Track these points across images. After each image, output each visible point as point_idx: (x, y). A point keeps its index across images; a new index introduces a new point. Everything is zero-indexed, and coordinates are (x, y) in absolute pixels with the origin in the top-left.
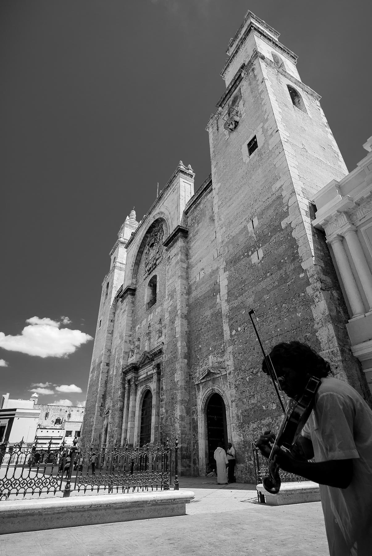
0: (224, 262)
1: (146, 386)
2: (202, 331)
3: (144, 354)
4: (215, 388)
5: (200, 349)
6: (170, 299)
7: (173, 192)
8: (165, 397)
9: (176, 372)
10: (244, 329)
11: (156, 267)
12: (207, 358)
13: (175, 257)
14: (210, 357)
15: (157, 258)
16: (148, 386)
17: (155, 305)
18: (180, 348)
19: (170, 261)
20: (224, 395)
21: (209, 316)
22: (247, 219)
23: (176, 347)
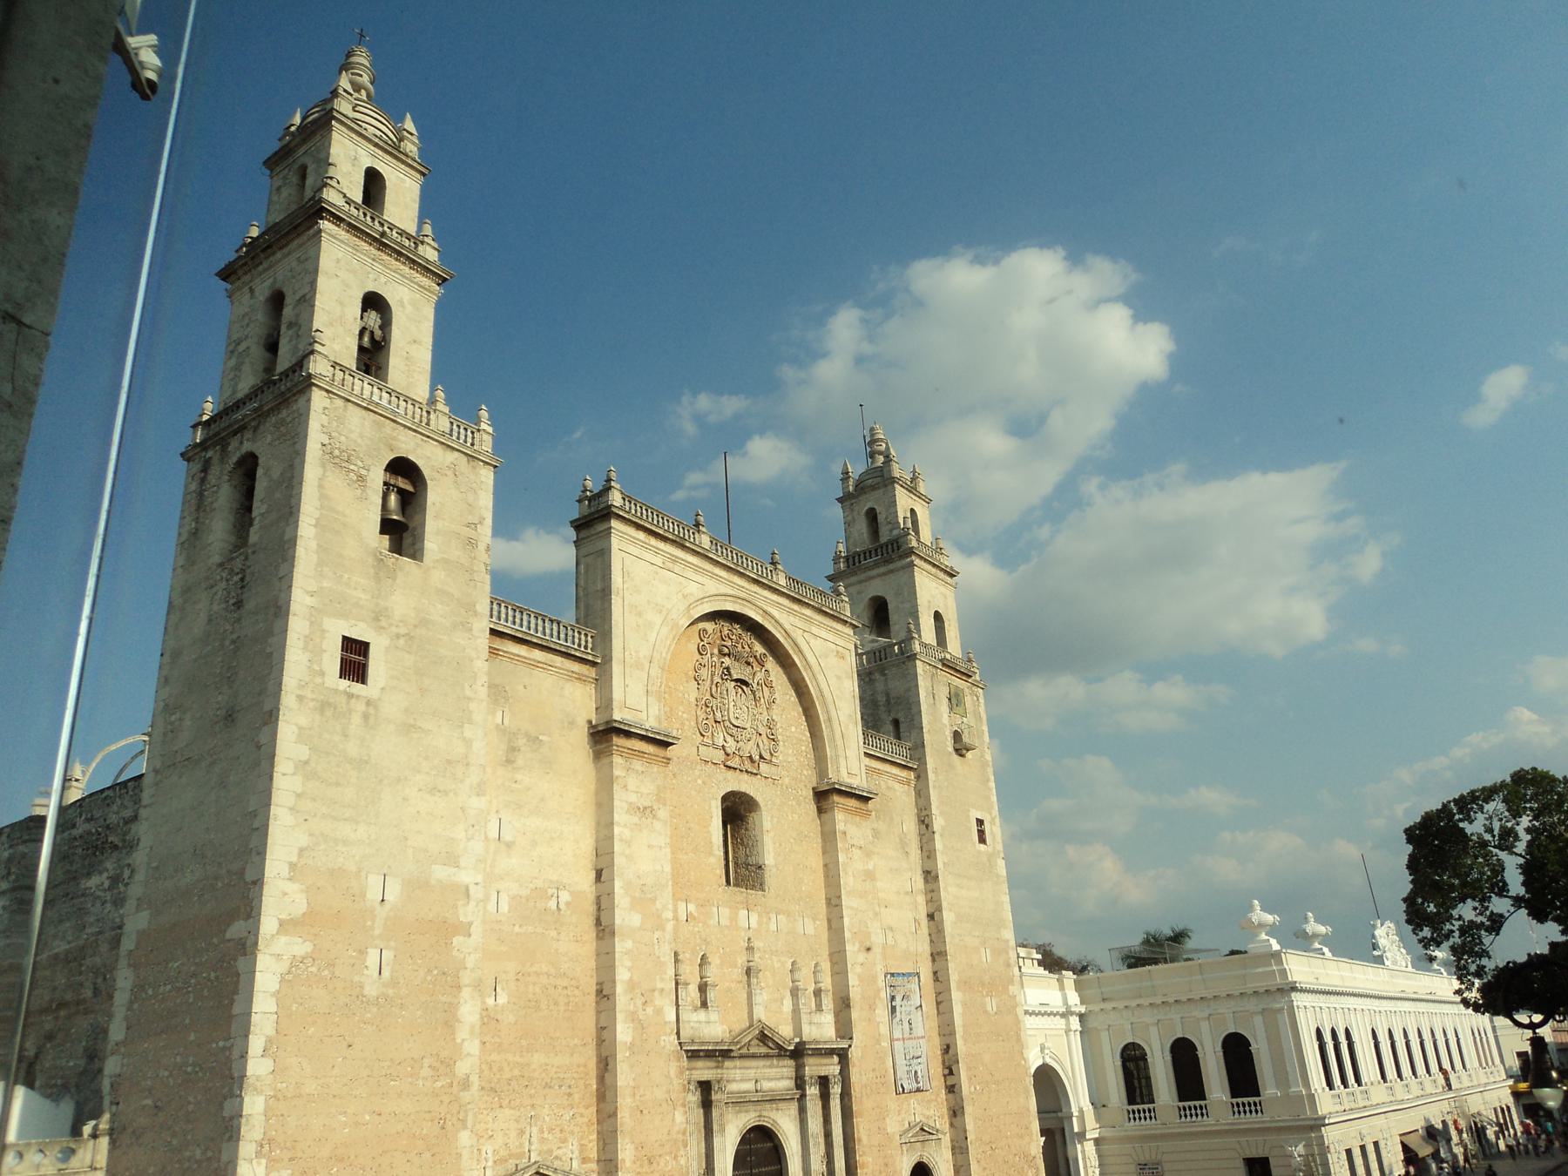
6: (857, 945)
8: (870, 1159)
9: (888, 1115)
11: (757, 774)
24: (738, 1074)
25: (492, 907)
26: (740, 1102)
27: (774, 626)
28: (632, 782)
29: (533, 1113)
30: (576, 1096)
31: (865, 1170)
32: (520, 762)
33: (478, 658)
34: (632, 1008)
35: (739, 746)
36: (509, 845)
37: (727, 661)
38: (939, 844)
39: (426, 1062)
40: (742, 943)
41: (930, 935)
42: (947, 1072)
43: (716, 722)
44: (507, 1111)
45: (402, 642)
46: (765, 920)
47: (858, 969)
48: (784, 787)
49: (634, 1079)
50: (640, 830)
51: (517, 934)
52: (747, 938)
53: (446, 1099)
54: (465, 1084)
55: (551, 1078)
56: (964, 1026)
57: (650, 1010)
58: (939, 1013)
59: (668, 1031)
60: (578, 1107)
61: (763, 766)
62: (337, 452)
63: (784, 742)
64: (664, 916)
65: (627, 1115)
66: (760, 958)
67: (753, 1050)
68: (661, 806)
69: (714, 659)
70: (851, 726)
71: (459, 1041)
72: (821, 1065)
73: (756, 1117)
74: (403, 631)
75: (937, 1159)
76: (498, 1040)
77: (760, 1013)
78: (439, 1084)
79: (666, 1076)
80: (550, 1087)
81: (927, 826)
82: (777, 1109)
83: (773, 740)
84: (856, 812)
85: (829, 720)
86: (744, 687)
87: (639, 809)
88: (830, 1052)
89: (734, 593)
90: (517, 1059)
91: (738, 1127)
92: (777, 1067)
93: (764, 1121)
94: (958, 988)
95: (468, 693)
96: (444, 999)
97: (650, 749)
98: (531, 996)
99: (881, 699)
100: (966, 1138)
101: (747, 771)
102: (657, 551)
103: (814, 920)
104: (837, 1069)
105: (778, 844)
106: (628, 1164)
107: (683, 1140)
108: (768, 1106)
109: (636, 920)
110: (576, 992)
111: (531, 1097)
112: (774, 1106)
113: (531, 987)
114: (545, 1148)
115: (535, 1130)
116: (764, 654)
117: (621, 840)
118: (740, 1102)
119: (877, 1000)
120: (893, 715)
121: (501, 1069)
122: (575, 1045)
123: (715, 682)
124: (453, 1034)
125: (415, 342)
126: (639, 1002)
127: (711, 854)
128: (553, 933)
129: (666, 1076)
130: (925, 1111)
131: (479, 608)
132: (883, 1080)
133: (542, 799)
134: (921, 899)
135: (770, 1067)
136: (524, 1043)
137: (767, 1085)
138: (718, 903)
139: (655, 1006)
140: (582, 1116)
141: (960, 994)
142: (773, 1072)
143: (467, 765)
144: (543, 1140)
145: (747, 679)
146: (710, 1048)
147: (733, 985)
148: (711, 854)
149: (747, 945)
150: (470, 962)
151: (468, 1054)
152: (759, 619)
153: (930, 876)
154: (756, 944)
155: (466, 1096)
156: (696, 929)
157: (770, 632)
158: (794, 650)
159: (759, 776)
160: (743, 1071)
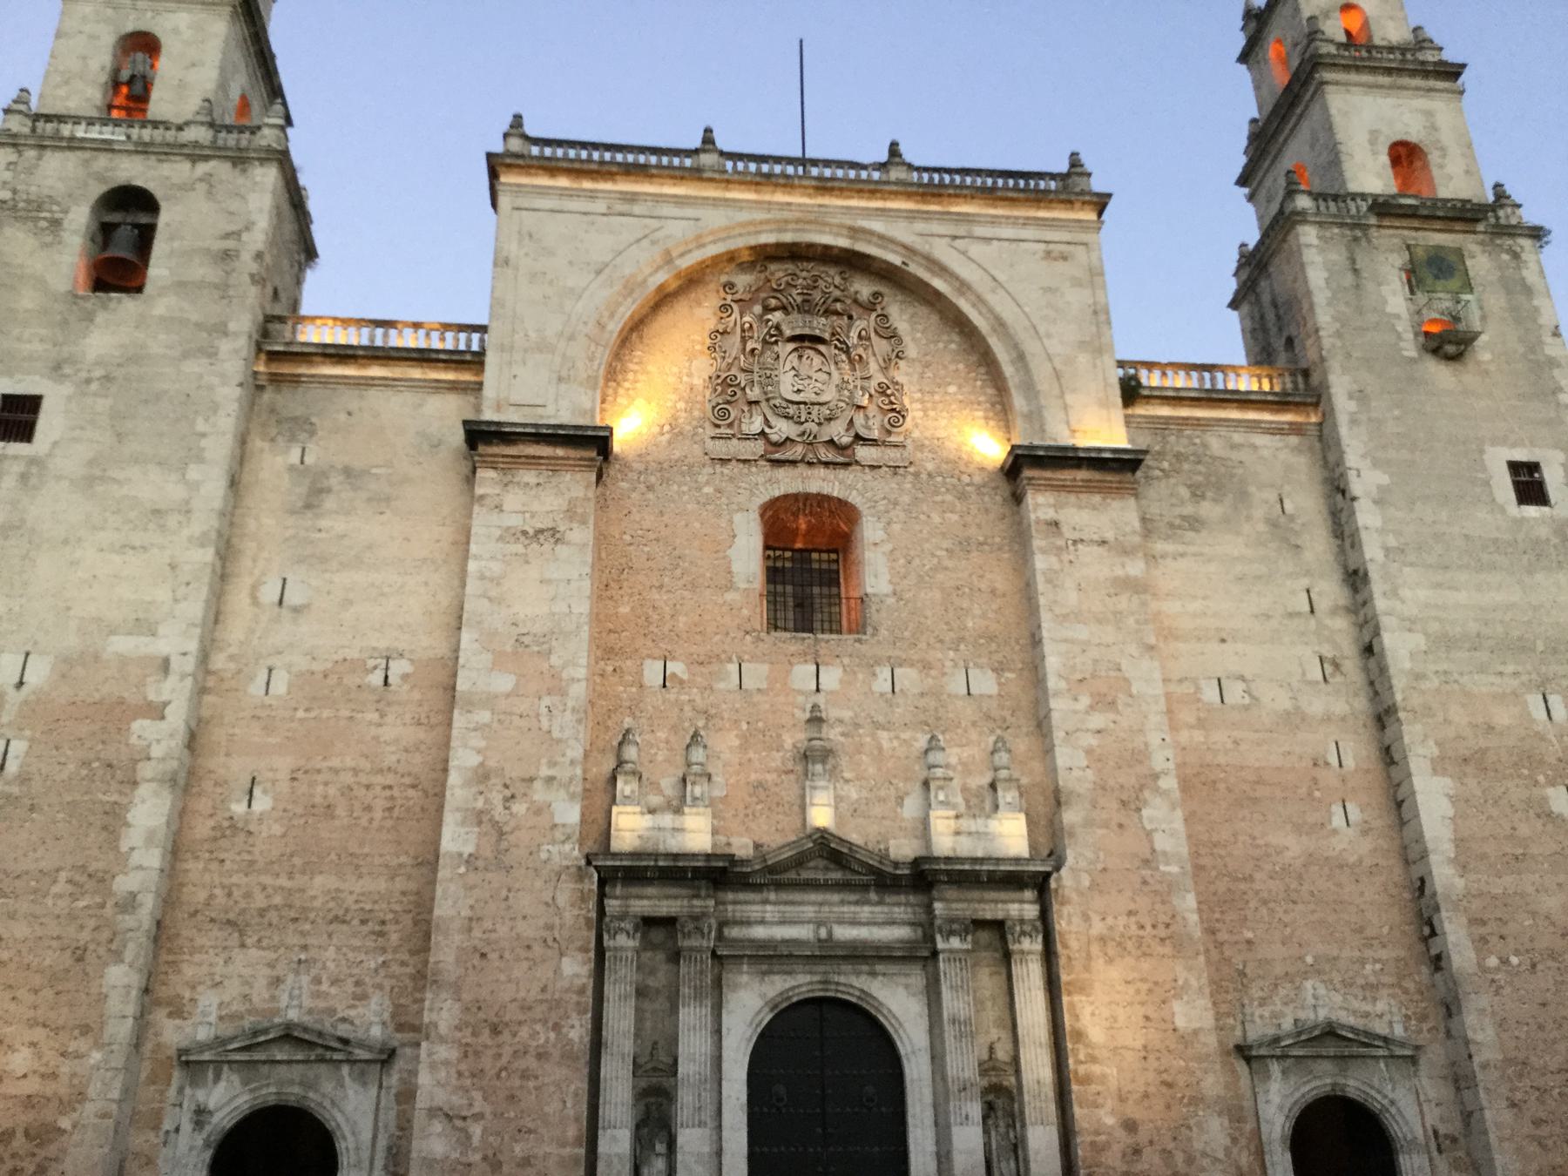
0: (1431, 743)
1: (820, 982)
2: (1257, 886)
4: (1351, 1082)
5: (1249, 942)
6: (1085, 701)
7: (1048, 255)
10: (1534, 966)
11: (846, 465)
12: (1292, 982)
13: (1096, 549)
14: (1308, 984)
15: (863, 433)
16: (838, 984)
17: (859, 641)
18: (1194, 918)
19: (1060, 542)
20: (1393, 1110)
21: (1289, 854)
22: (1525, 678)
23: (1163, 902)
24: (770, 911)
25: (257, 688)
26: (771, 957)
27: (880, 246)
28: (513, 499)
29: (303, 957)
30: (394, 938)
31: (1094, 1088)
32: (330, 503)
33: (224, 384)
34: (480, 804)
35: (802, 428)
36: (297, 610)
37: (777, 317)
38: (1366, 516)
39: (63, 876)
40: (798, 713)
41: (1372, 683)
42: (1427, 931)
43: (750, 403)
44: (253, 952)
45: (94, 386)
47: (1092, 741)
48: (924, 476)
49: (472, 907)
50: (527, 562)
51: (301, 720)
52: (809, 707)
53: (92, 923)
54: (129, 903)
55: (347, 910)
56: (1459, 842)
57: (519, 808)
58: (1402, 823)
59: (559, 835)
60: (395, 950)
61: (863, 453)
62: (21, 205)
64: (565, 675)
65: (451, 959)
66: (843, 734)
67: (806, 875)
68: (575, 525)
69: (747, 319)
70: (1083, 359)
71: (124, 848)
72: (981, 901)
73: (811, 983)
74: (98, 373)
75: (1391, 1095)
76: (246, 857)
77: (821, 816)
78: (81, 904)
79: (547, 904)
80: (344, 922)
81: (1343, 492)
82: (873, 974)
83: (893, 410)
84: (1088, 487)
85: (1021, 358)
86: (822, 348)
87: (524, 533)
88: (1010, 879)
89: (769, 216)
90: (283, 881)
91: (762, 996)
92: (880, 903)
94: (1435, 772)
95: (201, 426)
96: (105, 798)
97: (560, 452)
98: (318, 800)
99: (1270, 316)
100: (1470, 1057)
101: (820, 462)
102: (592, 195)
103: (998, 670)
104: (1031, 911)
105: (902, 561)
106: (443, 1028)
107: (578, 1003)
109: (503, 683)
110: (411, 793)
111: (303, 934)
112: (865, 968)
113: (320, 789)
114: (322, 1004)
115: (305, 980)
116: (876, 295)
117: (482, 577)
118: (771, 957)
119: (1147, 794)
120: (1285, 334)
121: (248, 895)
122: (400, 866)
124: (117, 839)
125: (193, 65)
126: (497, 798)
127: (730, 586)
128: (375, 716)
129: (547, 904)
130: (1356, 1004)
131: (232, 326)
132: (1162, 932)
133: (370, 547)
134: (1341, 624)
135: (857, 903)
136: (297, 861)
137: (843, 933)
138: (739, 658)
139: (533, 802)
140: (403, 964)
141: (1444, 783)
142: (865, 912)
143: (188, 512)
144: (317, 995)
145: (817, 332)
146: (661, 863)
147: (771, 777)
148: (730, 586)
149: (808, 715)
150: (156, 751)
151: (140, 868)
152: (843, 242)
153: (1356, 579)
154: (831, 713)
155: (128, 921)
156: (685, 698)
157: (868, 257)
158: (928, 269)
159: (854, 467)
160: (782, 908)
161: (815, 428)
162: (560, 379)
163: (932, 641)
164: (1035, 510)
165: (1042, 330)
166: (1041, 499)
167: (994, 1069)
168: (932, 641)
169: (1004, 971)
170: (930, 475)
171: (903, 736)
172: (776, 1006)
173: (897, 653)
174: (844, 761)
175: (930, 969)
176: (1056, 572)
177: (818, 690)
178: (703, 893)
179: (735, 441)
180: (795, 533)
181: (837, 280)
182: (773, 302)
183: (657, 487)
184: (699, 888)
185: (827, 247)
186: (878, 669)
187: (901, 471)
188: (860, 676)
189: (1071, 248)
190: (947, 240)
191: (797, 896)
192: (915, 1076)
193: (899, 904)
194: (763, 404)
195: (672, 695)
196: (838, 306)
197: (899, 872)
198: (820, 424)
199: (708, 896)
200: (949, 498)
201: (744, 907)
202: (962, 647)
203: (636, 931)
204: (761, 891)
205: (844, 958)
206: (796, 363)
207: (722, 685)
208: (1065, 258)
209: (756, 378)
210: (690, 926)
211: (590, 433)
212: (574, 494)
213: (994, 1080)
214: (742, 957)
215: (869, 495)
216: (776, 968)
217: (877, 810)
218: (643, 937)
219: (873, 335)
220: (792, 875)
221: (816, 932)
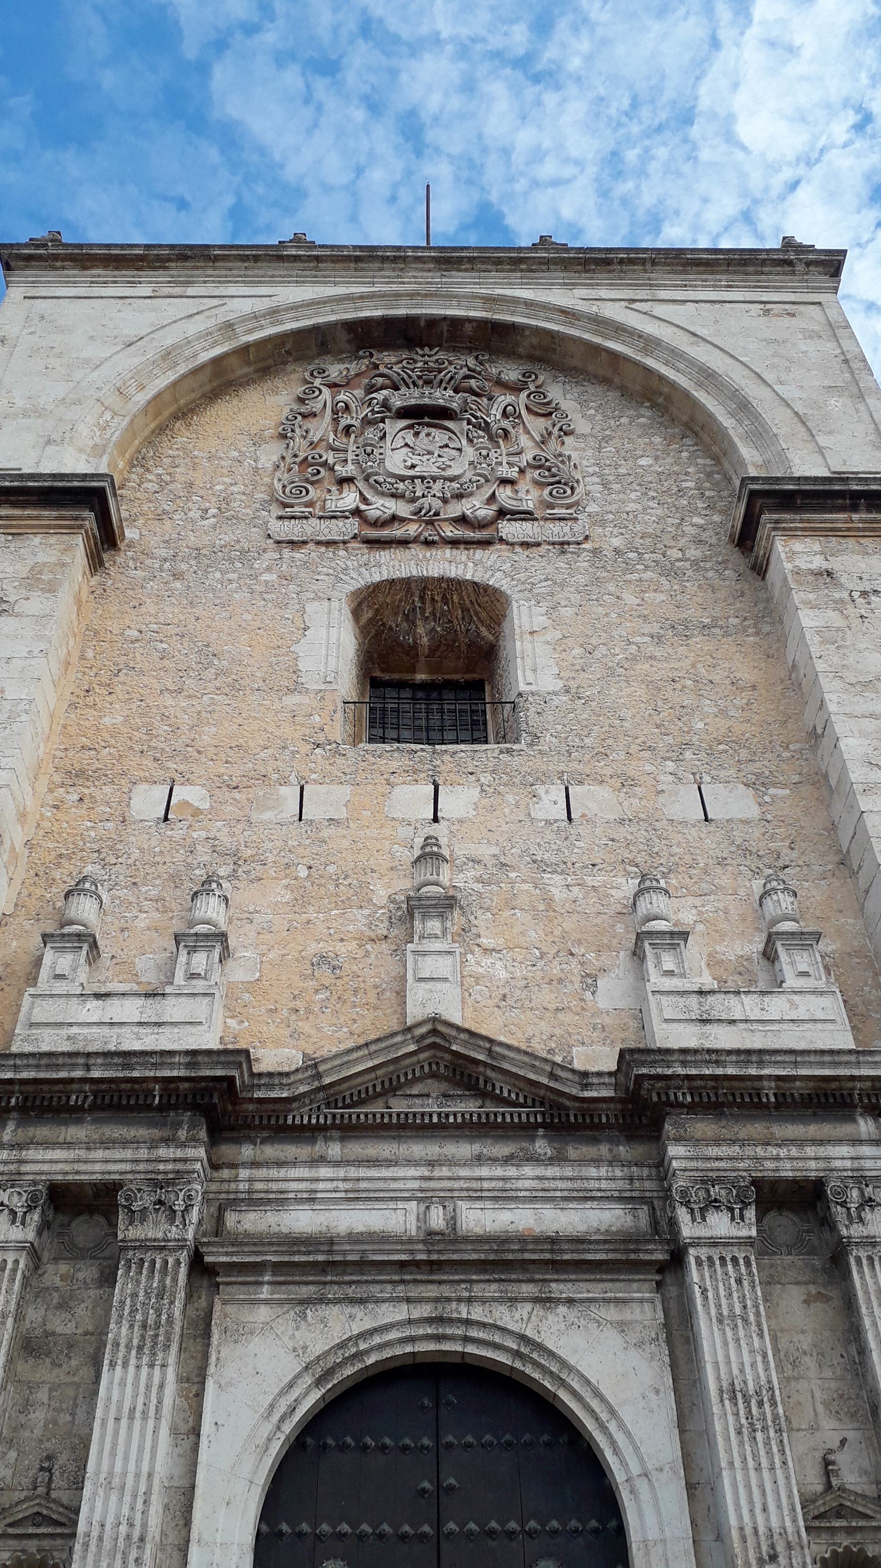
1: (429, 1321)
3: (423, 1030)
11: (486, 543)
16: (468, 1322)
17: (509, 751)
46: (510, 798)
48: (610, 554)
52: (419, 841)
63: (605, 485)
66: (479, 880)
67: (399, 1106)
69: (341, 397)
70: (836, 404)
82: (546, 1302)
83: (559, 482)
86: (450, 424)
93: (466, 1339)
105: (577, 651)
108: (492, 1290)
123: (340, 428)
135: (508, 1160)
146: (96, 1074)
147: (342, 949)
149: (417, 852)
160: (353, 1172)
161: (437, 504)
162: (49, 442)
163: (634, 749)
164: (790, 559)
165: (769, 377)
166: (797, 546)
167: (839, 1512)
168: (634, 749)
169: (834, 1293)
170: (617, 551)
171: (589, 881)
172: (329, 1373)
173: (575, 765)
174: (482, 920)
175: (672, 1291)
176: (838, 629)
177: (436, 819)
178: (182, 1134)
179: (314, 521)
180: (412, 650)
181: (471, 362)
182: (380, 380)
183: (188, 576)
184: (177, 1125)
185: (455, 322)
186: (540, 789)
187: (572, 548)
188: (510, 798)
189: (795, 307)
190: (624, 304)
191: (385, 1149)
192: (653, 1534)
193: (596, 1162)
194: (361, 484)
195: (177, 832)
196: (473, 383)
197: (587, 1094)
198: (445, 501)
199: (193, 1141)
200: (649, 575)
201: (274, 1173)
202: (688, 755)
203: (30, 1209)
204: (313, 1141)
205: (483, 1266)
206: (410, 440)
207: (268, 815)
208: (793, 315)
209: (350, 456)
210: (146, 1200)
211: (76, 484)
212: (41, 558)
213: (846, 1541)
214: (257, 1268)
215: (522, 576)
216: (332, 1292)
217: (546, 997)
218: (44, 1227)
219: (524, 412)
220: (377, 1108)
221: (422, 1218)
